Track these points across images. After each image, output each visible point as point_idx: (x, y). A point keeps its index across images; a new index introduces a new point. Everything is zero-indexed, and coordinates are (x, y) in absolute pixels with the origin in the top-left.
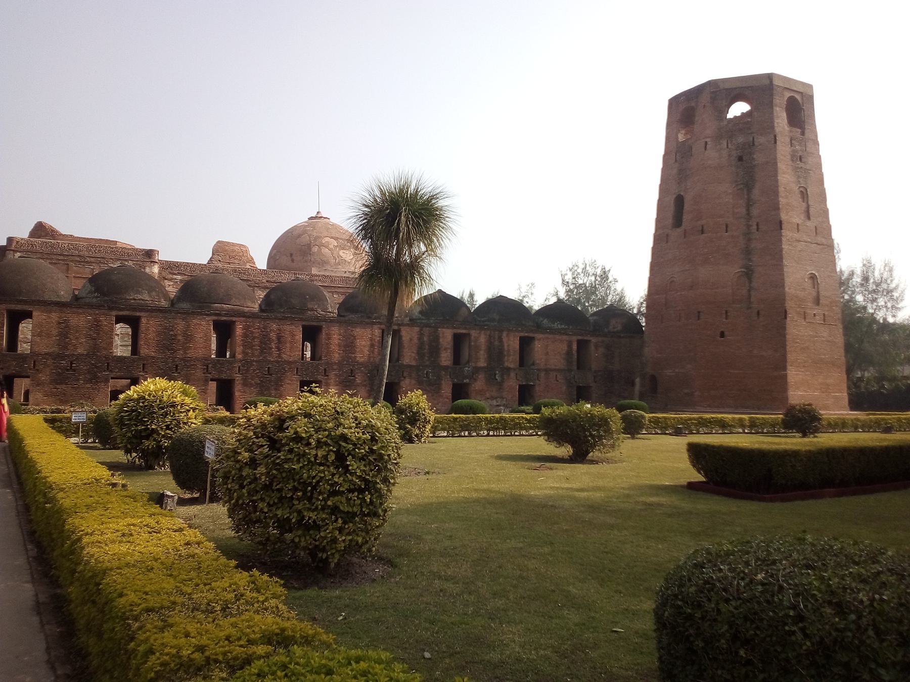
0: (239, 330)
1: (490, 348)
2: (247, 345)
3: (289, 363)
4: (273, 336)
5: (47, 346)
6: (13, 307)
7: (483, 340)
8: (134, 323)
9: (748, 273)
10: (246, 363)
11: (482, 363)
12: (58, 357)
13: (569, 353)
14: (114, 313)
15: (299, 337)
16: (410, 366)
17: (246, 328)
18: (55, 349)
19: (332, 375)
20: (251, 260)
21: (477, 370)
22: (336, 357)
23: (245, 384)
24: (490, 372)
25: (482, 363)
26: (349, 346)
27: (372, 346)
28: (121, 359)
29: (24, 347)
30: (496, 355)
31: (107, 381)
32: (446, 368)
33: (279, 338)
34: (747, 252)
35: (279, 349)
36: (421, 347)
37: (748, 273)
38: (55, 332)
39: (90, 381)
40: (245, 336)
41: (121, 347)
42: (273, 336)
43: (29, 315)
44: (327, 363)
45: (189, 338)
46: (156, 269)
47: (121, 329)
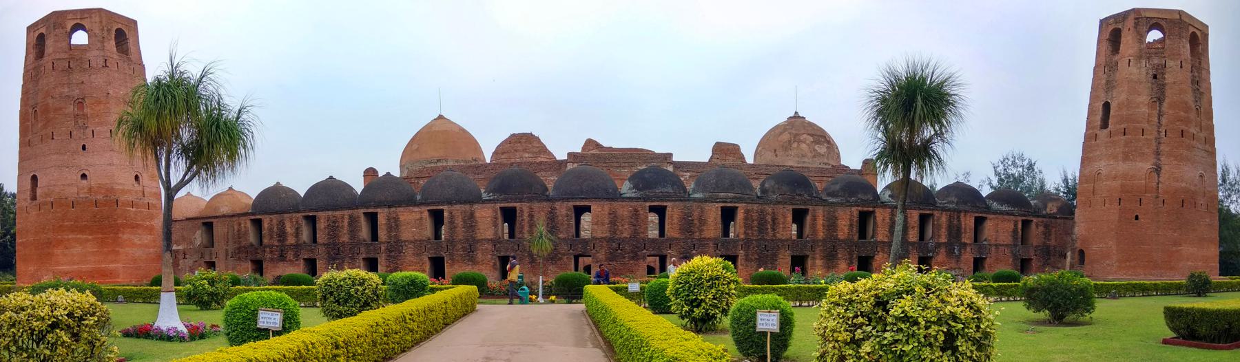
0: (740, 215)
2: (748, 226)
3: (781, 240)
4: (769, 218)
5: (603, 232)
6: (578, 203)
8: (660, 211)
10: (747, 243)
12: (610, 240)
14: (648, 204)
15: (790, 218)
16: (884, 242)
17: (747, 212)
18: (608, 235)
19: (818, 250)
20: (742, 157)
22: (821, 235)
23: (746, 260)
26: (832, 225)
27: (851, 225)
28: (653, 240)
29: (585, 234)
31: (644, 258)
33: (774, 220)
35: (774, 229)
38: (607, 221)
39: (633, 258)
40: (746, 219)
41: (653, 233)
42: (769, 218)
43: (588, 209)
44: (814, 241)
45: (703, 222)
47: (653, 218)
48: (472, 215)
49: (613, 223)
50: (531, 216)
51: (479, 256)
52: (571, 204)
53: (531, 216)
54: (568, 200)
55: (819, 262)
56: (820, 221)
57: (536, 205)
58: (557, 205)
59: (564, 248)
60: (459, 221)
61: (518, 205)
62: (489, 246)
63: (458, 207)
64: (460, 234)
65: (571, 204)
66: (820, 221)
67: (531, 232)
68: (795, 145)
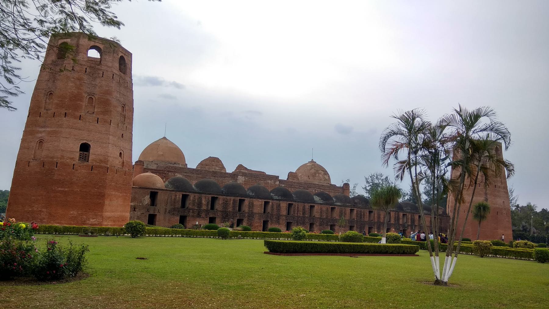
1: (411, 219)
7: (410, 216)
9: (486, 200)
11: (410, 224)
12: (320, 218)
13: (431, 221)
17: (357, 211)
21: (408, 225)
22: (376, 220)
24: (411, 226)
25: (410, 224)
26: (379, 217)
30: (413, 221)
32: (401, 225)
34: (486, 194)
36: (395, 218)
37: (486, 200)
46: (278, 183)
48: (279, 205)
49: (321, 212)
50: (298, 208)
51: (281, 221)
52: (310, 204)
53: (298, 208)
54: (309, 203)
55: (376, 230)
56: (376, 216)
57: (300, 204)
58: (306, 204)
59: (307, 220)
60: (275, 207)
61: (294, 203)
62: (284, 218)
63: (275, 201)
64: (275, 212)
65: (310, 204)
66: (376, 216)
67: (297, 214)
68: (317, 175)
